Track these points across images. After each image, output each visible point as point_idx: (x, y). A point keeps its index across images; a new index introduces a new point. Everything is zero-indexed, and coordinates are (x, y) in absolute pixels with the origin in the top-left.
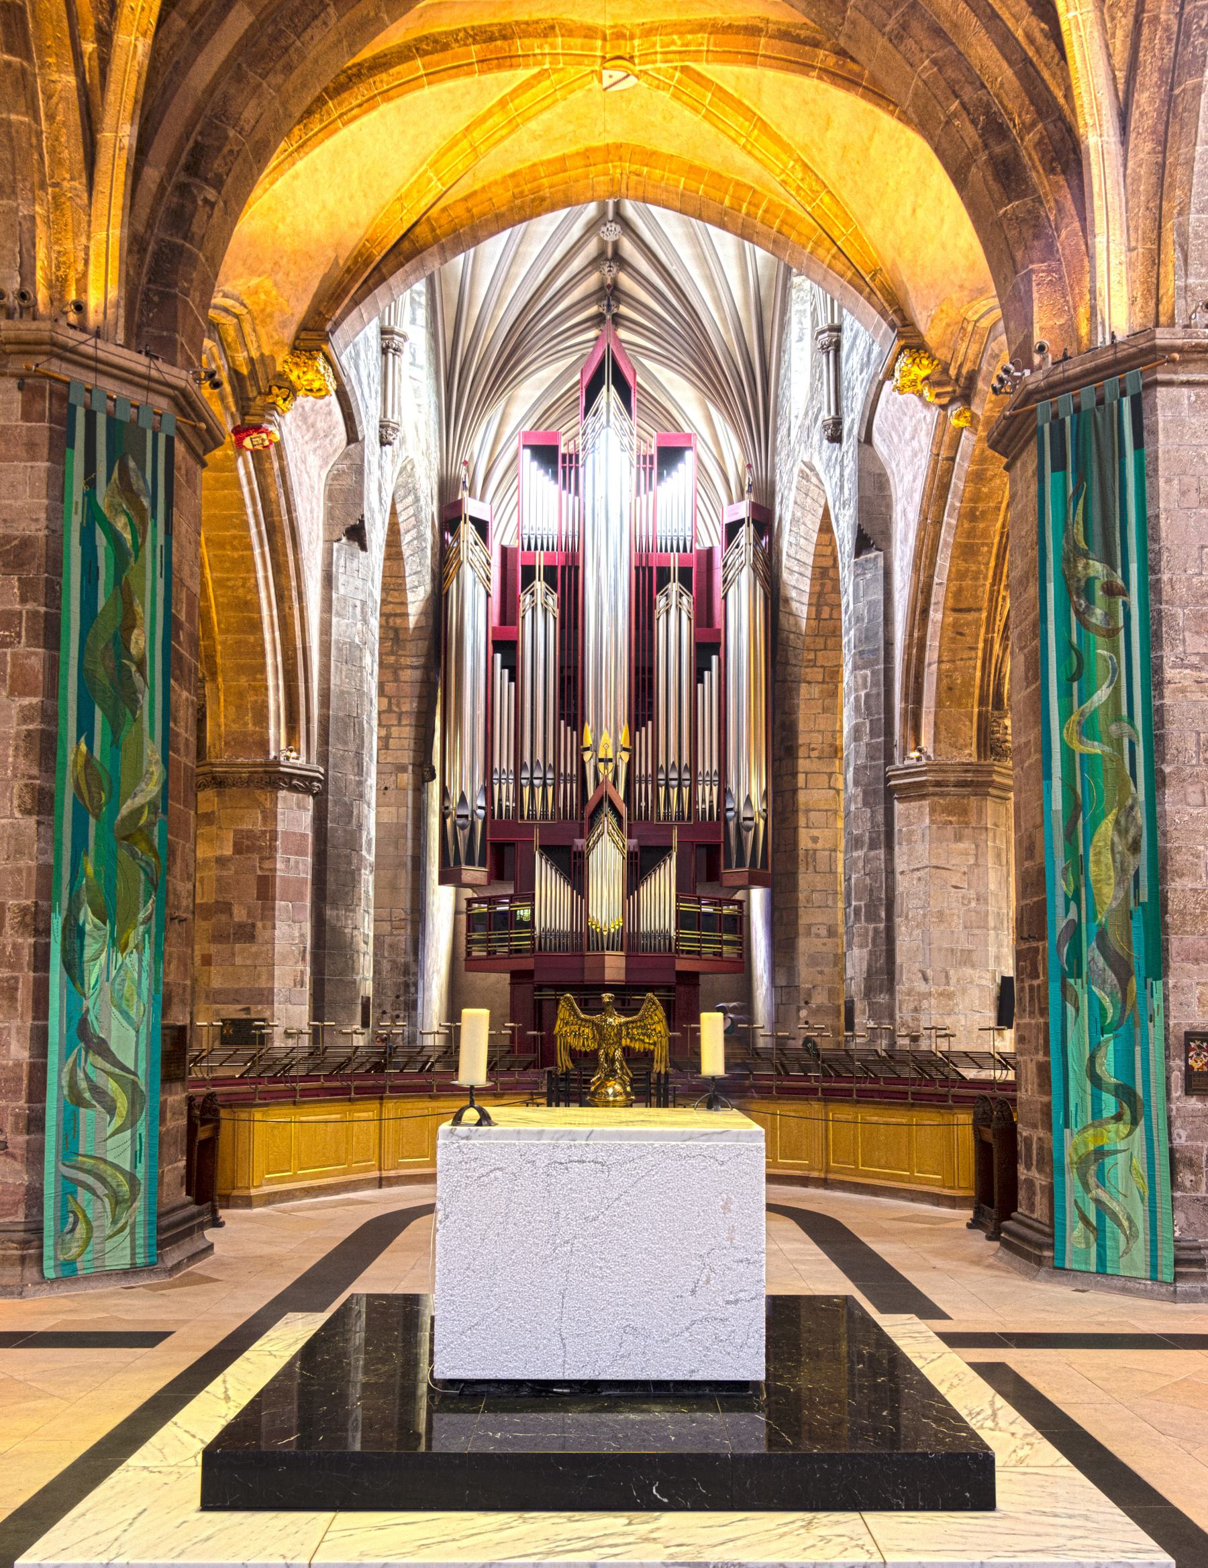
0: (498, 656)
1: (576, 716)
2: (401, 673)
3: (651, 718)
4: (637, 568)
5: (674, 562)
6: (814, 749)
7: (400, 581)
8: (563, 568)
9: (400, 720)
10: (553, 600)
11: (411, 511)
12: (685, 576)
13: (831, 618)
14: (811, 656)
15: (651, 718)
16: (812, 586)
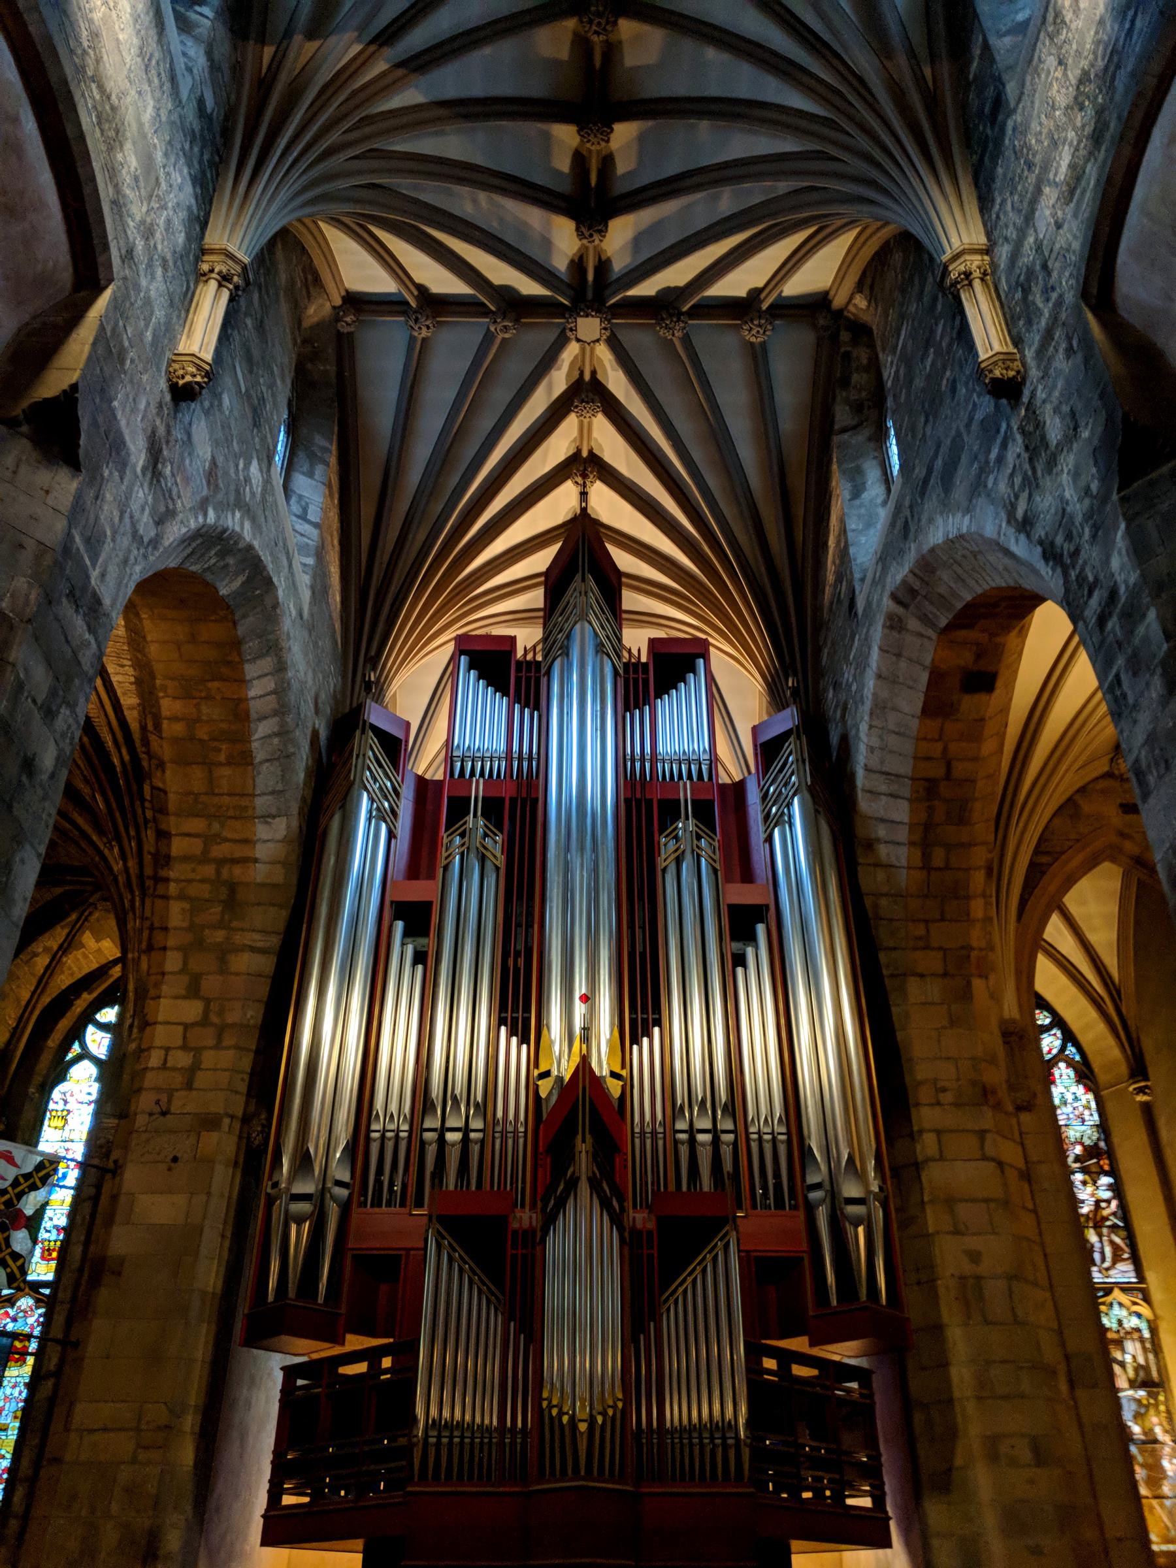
0: (399, 926)
1: (527, 1021)
2: (232, 958)
3: (658, 1022)
4: (628, 801)
5: (686, 793)
6: (944, 1090)
7: (244, 802)
8: (513, 801)
9: (220, 1037)
10: (496, 846)
11: (270, 684)
12: (703, 811)
13: (947, 867)
14: (920, 930)
15: (658, 1022)
16: (912, 811)
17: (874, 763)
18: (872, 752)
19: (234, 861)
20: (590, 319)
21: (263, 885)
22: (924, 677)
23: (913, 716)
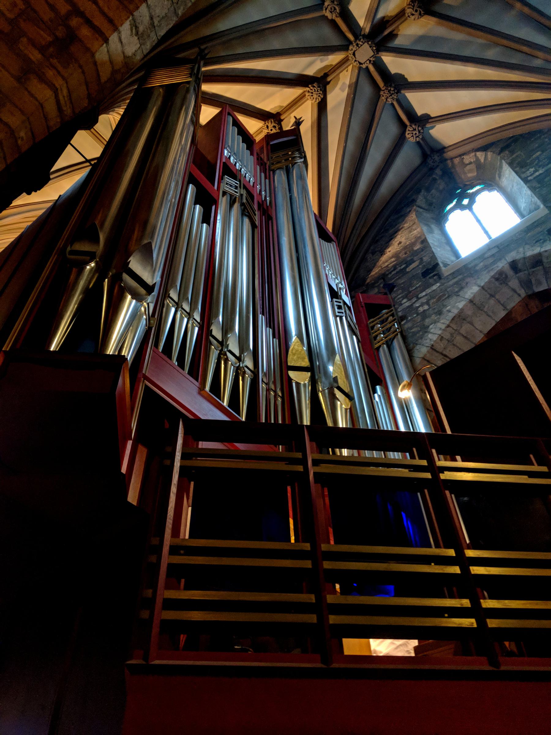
17: (440, 347)
18: (441, 340)
19: (89, 22)
20: (370, 49)
21: (95, 63)
22: (502, 314)
23: (481, 332)
